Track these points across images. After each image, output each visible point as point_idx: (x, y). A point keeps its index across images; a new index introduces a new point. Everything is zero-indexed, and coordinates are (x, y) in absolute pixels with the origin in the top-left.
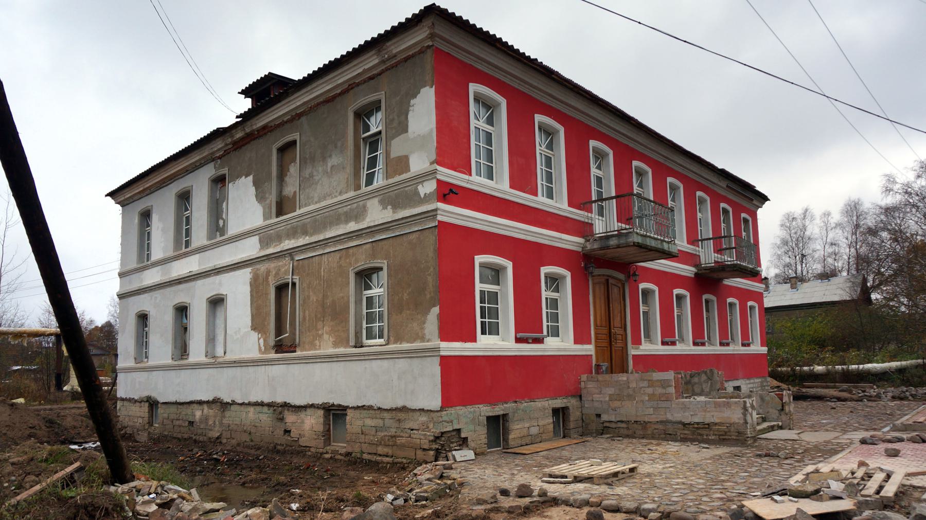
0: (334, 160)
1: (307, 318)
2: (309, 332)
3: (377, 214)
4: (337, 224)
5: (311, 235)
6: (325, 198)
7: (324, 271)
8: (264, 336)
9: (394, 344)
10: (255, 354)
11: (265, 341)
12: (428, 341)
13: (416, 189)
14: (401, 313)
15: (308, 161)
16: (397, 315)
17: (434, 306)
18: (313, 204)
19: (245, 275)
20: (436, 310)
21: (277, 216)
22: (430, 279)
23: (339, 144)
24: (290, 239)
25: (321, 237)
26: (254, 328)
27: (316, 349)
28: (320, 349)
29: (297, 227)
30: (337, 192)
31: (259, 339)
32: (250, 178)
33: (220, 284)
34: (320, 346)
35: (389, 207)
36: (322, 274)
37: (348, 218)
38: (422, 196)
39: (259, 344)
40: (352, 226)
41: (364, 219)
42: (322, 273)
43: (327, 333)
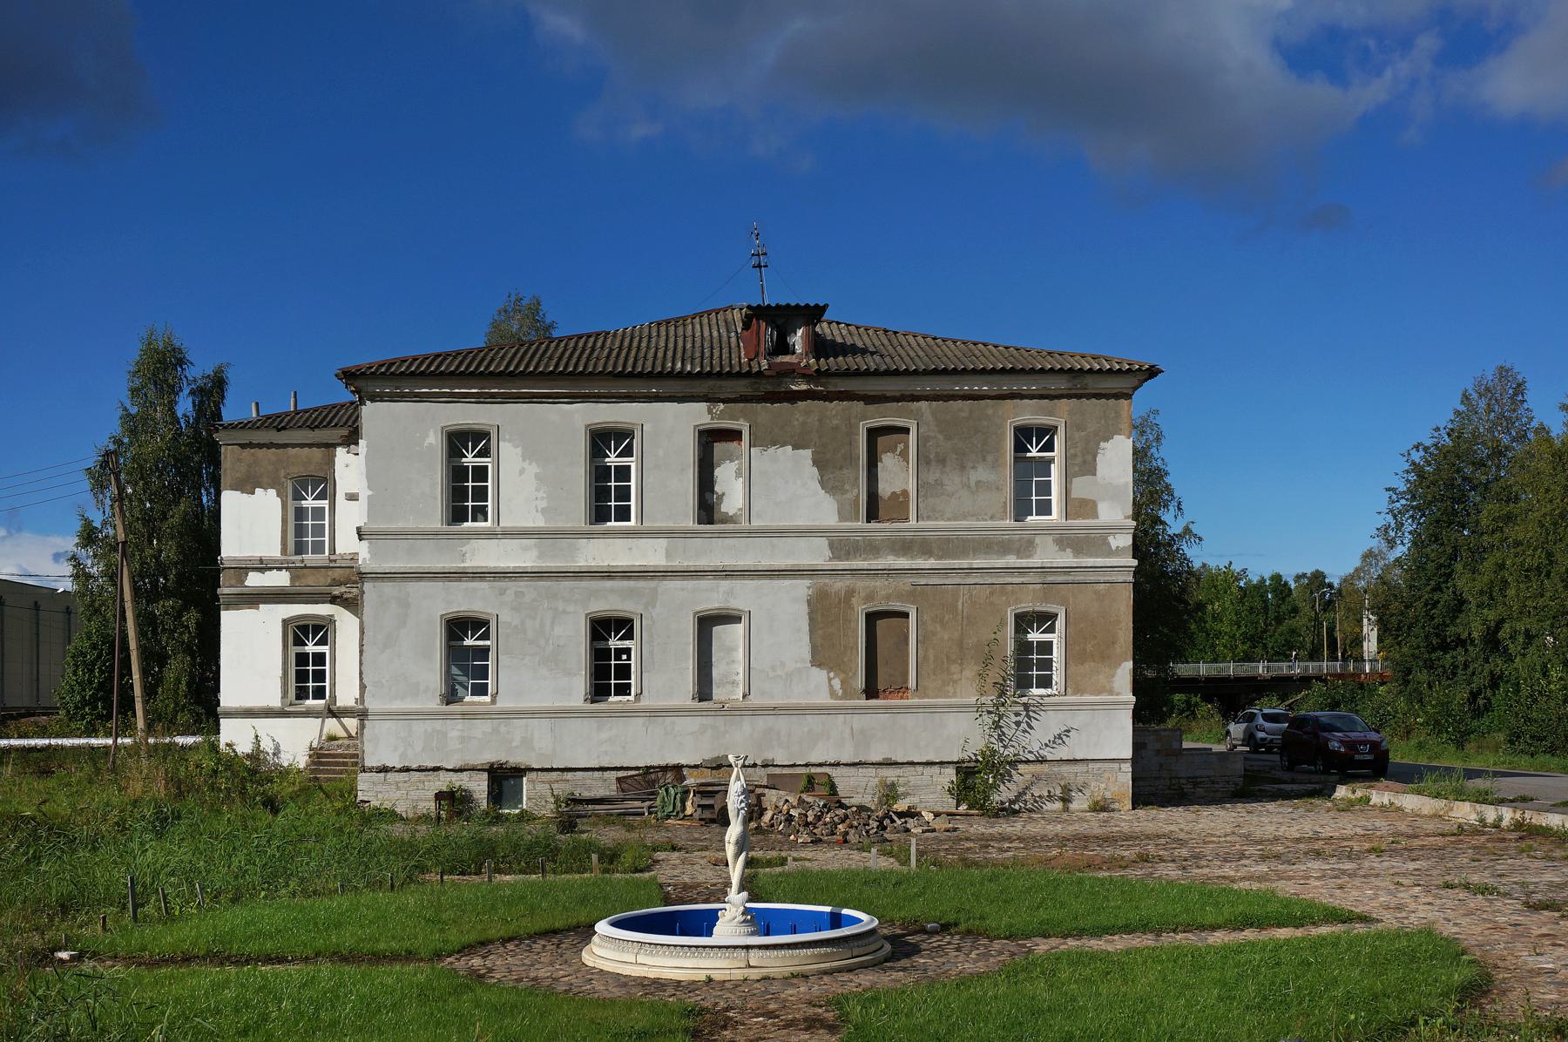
0: (980, 474)
1: (932, 658)
2: (934, 674)
3: (1048, 555)
4: (986, 553)
5: (940, 558)
6: (965, 518)
7: (963, 604)
8: (842, 676)
9: (1072, 695)
10: (824, 699)
11: (843, 682)
12: (1117, 695)
13: (1106, 539)
14: (1082, 664)
15: (933, 463)
16: (1076, 665)
17: (1126, 660)
18: (943, 519)
19: (802, 587)
20: (1129, 665)
21: (868, 521)
22: (1121, 633)
23: (990, 458)
24: (897, 555)
25: (964, 563)
26: (818, 660)
27: (946, 697)
28: (955, 693)
29: (912, 541)
30: (986, 514)
31: (830, 680)
32: (807, 454)
33: (730, 593)
34: (955, 692)
35: (1068, 550)
36: (960, 607)
37: (1019, 553)
38: (1114, 548)
39: (831, 686)
40: (1012, 560)
41: (1029, 556)
42: (960, 607)
43: (968, 679)
